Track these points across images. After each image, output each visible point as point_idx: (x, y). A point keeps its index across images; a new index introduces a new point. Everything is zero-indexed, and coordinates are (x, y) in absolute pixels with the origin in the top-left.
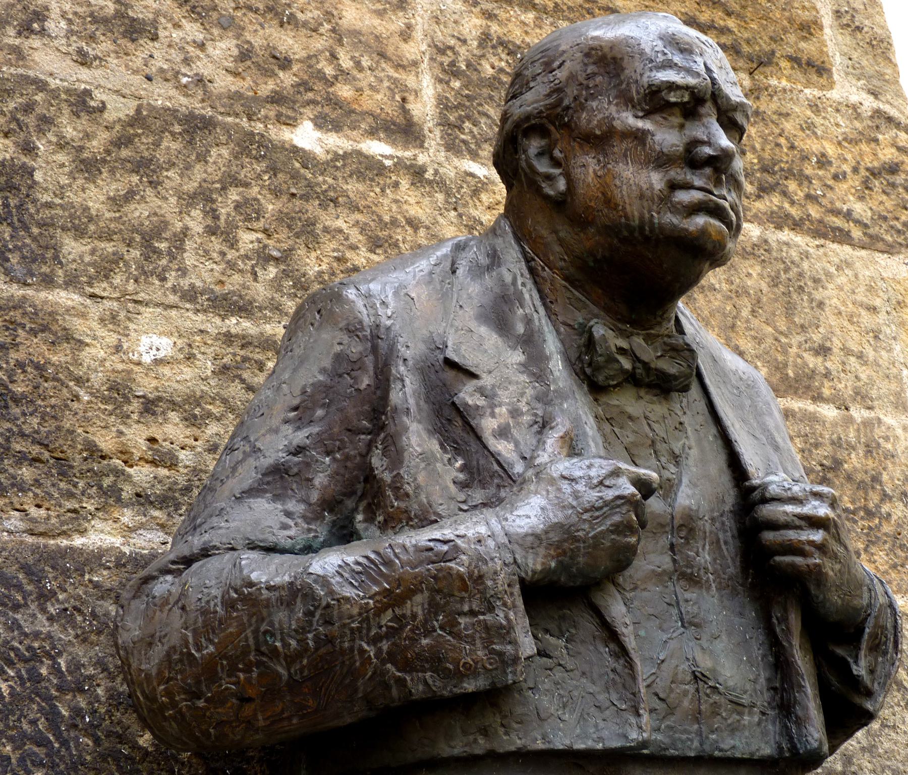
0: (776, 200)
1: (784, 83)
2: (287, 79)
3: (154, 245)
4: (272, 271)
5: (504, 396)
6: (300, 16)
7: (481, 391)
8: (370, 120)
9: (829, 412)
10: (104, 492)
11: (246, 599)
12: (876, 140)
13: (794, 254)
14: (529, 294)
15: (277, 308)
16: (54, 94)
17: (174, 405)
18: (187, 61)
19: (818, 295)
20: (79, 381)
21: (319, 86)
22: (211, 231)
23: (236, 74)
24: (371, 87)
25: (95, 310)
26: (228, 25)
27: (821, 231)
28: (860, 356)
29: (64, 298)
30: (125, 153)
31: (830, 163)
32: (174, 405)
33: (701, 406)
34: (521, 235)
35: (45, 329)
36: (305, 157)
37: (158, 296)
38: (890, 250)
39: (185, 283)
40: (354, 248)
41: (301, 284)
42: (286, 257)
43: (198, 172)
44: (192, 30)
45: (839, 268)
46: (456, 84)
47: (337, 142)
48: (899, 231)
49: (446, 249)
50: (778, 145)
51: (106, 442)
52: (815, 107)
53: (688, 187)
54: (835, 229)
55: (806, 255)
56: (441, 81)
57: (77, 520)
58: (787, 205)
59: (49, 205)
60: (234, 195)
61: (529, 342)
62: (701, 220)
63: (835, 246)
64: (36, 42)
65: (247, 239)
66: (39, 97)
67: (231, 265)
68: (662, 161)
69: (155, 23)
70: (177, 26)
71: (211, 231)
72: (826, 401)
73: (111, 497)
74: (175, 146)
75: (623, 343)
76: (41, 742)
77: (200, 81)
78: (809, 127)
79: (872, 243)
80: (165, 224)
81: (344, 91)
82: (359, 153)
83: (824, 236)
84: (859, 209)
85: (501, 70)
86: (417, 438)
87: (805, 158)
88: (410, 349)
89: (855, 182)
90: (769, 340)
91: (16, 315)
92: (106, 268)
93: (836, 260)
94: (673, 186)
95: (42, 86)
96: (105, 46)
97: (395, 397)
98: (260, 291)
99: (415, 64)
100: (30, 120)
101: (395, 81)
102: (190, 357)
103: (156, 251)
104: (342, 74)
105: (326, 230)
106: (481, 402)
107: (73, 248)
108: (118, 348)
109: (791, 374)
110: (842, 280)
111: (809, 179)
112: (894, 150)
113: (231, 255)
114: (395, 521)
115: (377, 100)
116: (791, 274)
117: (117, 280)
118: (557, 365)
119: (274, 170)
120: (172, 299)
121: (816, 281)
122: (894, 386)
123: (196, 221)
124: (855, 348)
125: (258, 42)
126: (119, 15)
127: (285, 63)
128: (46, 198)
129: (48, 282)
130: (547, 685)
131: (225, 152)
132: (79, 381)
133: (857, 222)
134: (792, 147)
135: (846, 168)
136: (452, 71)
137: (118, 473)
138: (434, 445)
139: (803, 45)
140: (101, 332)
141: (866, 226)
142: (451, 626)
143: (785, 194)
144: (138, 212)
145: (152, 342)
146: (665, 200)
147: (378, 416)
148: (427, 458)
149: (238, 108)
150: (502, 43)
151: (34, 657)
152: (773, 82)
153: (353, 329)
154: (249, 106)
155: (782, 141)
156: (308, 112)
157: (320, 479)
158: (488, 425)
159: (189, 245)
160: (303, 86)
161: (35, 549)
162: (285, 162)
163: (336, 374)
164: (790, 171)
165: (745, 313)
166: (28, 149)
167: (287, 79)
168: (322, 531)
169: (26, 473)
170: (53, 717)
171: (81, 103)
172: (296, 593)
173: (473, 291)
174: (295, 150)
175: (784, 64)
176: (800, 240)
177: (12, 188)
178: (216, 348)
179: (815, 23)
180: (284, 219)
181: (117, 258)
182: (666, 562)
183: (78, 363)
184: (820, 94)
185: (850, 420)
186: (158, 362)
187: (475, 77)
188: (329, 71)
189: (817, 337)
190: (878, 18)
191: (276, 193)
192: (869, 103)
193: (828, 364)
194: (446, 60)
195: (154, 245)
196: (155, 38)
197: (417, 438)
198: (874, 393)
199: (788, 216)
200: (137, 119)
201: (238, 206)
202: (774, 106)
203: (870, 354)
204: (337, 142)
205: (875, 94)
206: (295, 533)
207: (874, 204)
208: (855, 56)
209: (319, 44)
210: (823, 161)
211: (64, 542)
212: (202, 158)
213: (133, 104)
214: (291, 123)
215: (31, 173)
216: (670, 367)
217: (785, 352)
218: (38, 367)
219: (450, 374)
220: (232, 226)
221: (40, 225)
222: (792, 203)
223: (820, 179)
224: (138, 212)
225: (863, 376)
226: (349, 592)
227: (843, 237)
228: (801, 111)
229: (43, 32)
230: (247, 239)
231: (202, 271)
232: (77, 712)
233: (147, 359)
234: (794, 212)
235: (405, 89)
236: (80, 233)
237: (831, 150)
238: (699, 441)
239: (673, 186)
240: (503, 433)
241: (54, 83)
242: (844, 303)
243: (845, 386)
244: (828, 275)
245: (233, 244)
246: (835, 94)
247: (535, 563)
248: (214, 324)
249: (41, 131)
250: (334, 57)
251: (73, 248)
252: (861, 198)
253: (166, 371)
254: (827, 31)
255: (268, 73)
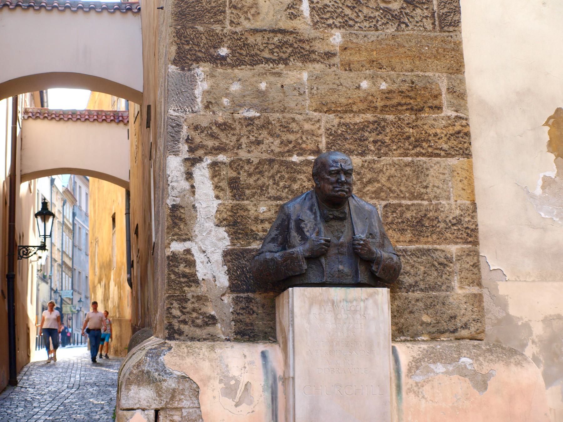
0: (418, 149)
1: (426, 115)
2: (291, 146)
3: (263, 188)
4: (287, 190)
5: (309, 225)
6: (294, 130)
7: (305, 224)
8: (309, 151)
9: (425, 203)
10: (254, 238)
11: (266, 261)
12: (454, 125)
13: (421, 163)
14: (316, 204)
15: (287, 198)
16: (243, 161)
17: (266, 220)
18: (269, 147)
19: (427, 173)
20: (249, 218)
21: (298, 146)
22: (274, 184)
23: (280, 147)
24: (310, 143)
25: (252, 204)
26: (278, 136)
27: (431, 155)
28: (438, 187)
29: (246, 202)
30: (257, 170)
31: (438, 135)
32: (266, 220)
33: (350, 221)
34: (316, 193)
35: (243, 209)
36: (294, 163)
37: (263, 199)
38: (453, 156)
39: (269, 196)
40: (304, 182)
41: (292, 192)
42: (290, 186)
43: (272, 172)
44: (271, 139)
45: (435, 164)
46: (331, 138)
47: (302, 158)
48: (457, 151)
49: (304, 195)
50: (422, 133)
51: (254, 229)
52: (435, 120)
53: (337, 187)
54: (435, 154)
55: (425, 163)
56: (327, 138)
57: (249, 244)
58: (421, 150)
59: (243, 184)
60: (279, 175)
61: (315, 214)
62: (340, 193)
63: (435, 159)
64: (240, 151)
65: (281, 184)
66: (241, 162)
67: (278, 190)
68: (332, 183)
69: (263, 141)
70: (268, 139)
71: (274, 184)
72: (425, 200)
73: (255, 239)
74: (267, 167)
75: (331, 213)
76: (245, 281)
77: (272, 151)
78: (433, 126)
79: (448, 155)
80: (265, 184)
81: (304, 146)
82: (307, 160)
83: (432, 156)
84: (445, 147)
85: (343, 131)
86: (294, 233)
87: (430, 135)
88: (293, 217)
89: (445, 139)
90: (410, 187)
91: (238, 207)
92: (253, 195)
93: (435, 162)
94: (334, 188)
95: (241, 160)
96: (253, 148)
97: (290, 226)
98: (284, 195)
99: (321, 135)
100: (239, 168)
101: (316, 140)
102: (270, 210)
103: (263, 190)
104: (304, 142)
105: (298, 179)
106: (304, 226)
107: (247, 192)
108: (256, 211)
109: (415, 194)
110: (435, 167)
111: (430, 141)
112: (460, 127)
113: (278, 188)
114: (290, 247)
115: (312, 146)
116: (419, 169)
117: (256, 197)
118: (319, 218)
119: (287, 168)
120: (266, 199)
121: (427, 169)
122: (447, 194)
123: (271, 182)
124: (436, 185)
125: (284, 138)
126: (256, 140)
127: (290, 142)
128: (243, 183)
129: (243, 200)
130: (311, 273)
131: (277, 166)
132: (249, 218)
133: (444, 150)
134: (426, 133)
135: (443, 135)
136: (331, 134)
137: (257, 234)
138: (296, 234)
139: (435, 102)
140: (253, 208)
141: (446, 151)
142: (294, 264)
143: (421, 147)
144: (260, 182)
145: (262, 208)
146: (333, 190)
147: (288, 229)
148: (294, 237)
149: (280, 155)
150: (343, 124)
151: (243, 268)
152: (423, 115)
153: (285, 214)
154: (282, 154)
155: (423, 132)
156: (296, 153)
157: (280, 240)
158: (305, 230)
159: (270, 187)
160: (295, 147)
161: (242, 249)
162: (290, 166)
163: (282, 222)
164: (424, 140)
165: (404, 181)
166: (239, 173)
167: (291, 146)
168: (280, 248)
169: (240, 236)
170: (246, 277)
171: (249, 162)
172: (272, 260)
173: (308, 204)
174: (293, 162)
175: (427, 109)
176: (424, 159)
177: (236, 182)
178: (275, 208)
179: (440, 94)
180: (289, 178)
181: (256, 192)
182: (337, 252)
183: (249, 214)
184: (436, 115)
185: (432, 204)
186: (264, 212)
187: (336, 134)
188: (300, 142)
189: (425, 184)
190: (463, 87)
191: (288, 173)
192: (454, 114)
193: (428, 190)
194: (329, 132)
195: (263, 188)
196: (263, 143)
197: (294, 233)
198: (440, 196)
199: (421, 153)
200: (260, 163)
201: (280, 177)
202: (422, 123)
203: (441, 186)
204: (302, 158)
205: (457, 111)
206: (276, 249)
207: (449, 144)
208: (452, 101)
209: (298, 135)
210: (436, 135)
211: (247, 247)
212: (272, 168)
213: (259, 159)
214: (291, 156)
215: (239, 178)
216: (340, 216)
217: (415, 189)
218: (242, 216)
219: (300, 221)
220: (278, 182)
221: (242, 188)
222: (423, 149)
223: (434, 140)
224: (260, 182)
225: (438, 192)
226: (280, 260)
227: (438, 155)
228: (431, 122)
229: (241, 148)
230: (281, 184)
231: (272, 192)
232: (250, 276)
233: (261, 212)
234: (424, 151)
235: (319, 142)
236: (249, 189)
237: (439, 131)
238: (348, 229)
239: (334, 188)
240: (308, 231)
241: (244, 158)
242: (435, 174)
243: (432, 195)
244: (431, 167)
245: (278, 185)
246: (443, 115)
247: (307, 254)
248: (274, 203)
249: (241, 169)
250: (302, 138)
251: (247, 192)
252: (446, 143)
253: (265, 214)
254: (444, 95)
255: (287, 145)
